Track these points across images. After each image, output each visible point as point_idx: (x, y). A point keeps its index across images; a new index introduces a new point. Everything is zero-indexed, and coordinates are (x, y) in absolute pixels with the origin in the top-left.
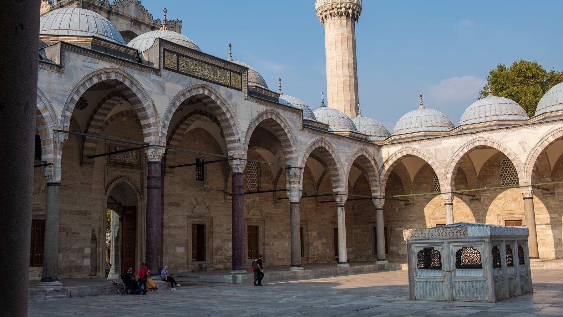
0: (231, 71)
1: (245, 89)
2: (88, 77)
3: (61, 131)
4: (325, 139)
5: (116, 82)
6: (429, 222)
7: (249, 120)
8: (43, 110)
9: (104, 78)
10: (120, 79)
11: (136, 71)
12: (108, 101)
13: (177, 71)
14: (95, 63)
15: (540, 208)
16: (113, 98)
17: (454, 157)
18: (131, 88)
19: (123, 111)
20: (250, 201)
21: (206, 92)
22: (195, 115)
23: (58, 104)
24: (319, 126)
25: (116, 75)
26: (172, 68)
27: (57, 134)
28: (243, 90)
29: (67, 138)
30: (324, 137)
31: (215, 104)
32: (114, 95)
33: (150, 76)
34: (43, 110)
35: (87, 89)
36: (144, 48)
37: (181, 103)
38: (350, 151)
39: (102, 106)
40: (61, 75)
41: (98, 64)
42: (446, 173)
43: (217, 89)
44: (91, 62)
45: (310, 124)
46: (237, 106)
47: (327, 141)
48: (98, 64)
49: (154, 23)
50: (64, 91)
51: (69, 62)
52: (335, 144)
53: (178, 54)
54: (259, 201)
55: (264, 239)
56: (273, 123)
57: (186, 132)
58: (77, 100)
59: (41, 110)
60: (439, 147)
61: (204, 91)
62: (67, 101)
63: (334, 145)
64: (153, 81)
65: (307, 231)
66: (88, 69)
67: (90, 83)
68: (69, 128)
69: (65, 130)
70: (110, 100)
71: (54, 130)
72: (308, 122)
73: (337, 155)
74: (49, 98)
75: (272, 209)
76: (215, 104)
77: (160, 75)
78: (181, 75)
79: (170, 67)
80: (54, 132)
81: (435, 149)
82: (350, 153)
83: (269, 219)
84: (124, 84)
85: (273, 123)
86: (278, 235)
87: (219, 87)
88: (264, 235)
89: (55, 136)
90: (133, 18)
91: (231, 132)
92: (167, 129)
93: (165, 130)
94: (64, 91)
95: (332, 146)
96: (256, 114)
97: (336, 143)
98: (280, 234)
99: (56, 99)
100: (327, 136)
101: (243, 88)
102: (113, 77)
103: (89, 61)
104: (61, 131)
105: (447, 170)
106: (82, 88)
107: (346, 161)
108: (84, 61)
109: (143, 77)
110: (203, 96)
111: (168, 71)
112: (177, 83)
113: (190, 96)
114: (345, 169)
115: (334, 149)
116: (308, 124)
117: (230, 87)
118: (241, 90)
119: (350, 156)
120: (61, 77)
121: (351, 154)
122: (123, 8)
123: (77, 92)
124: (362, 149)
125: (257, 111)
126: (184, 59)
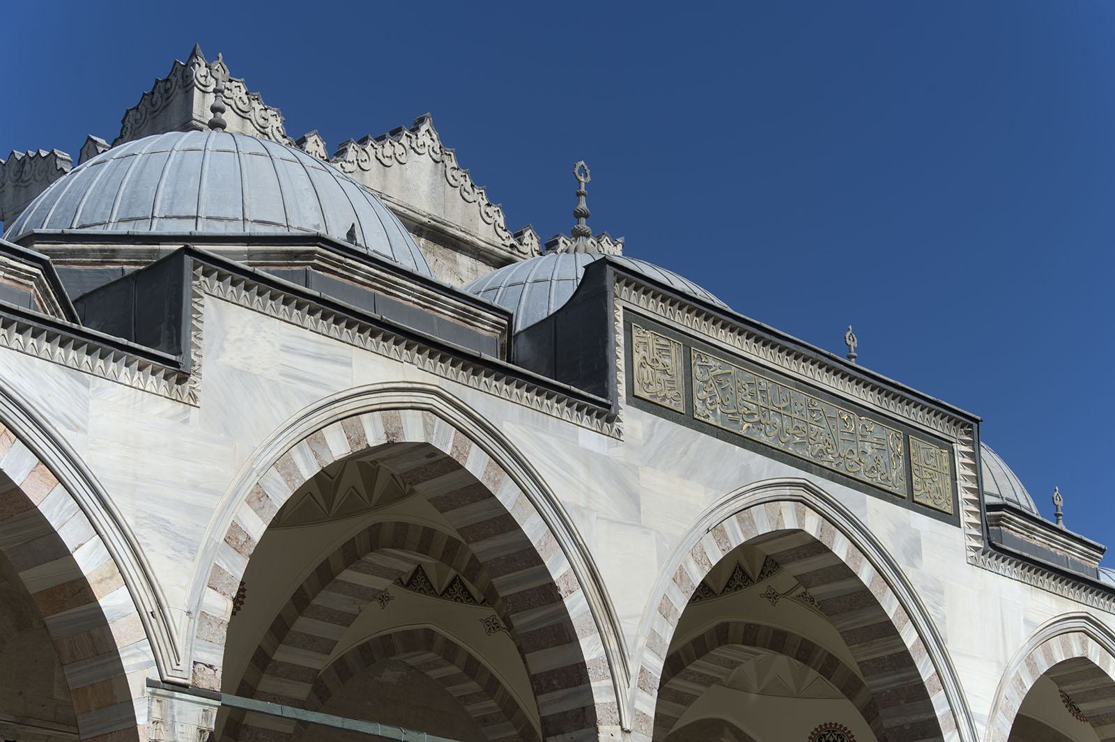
0: (908, 430)
1: (968, 516)
2: (305, 427)
3: (182, 688)
5: (424, 460)
7: (999, 663)
8: (100, 582)
9: (374, 434)
10: (446, 444)
11: (513, 410)
12: (348, 576)
13: (689, 419)
14: (334, 361)
16: (372, 558)
18: (490, 488)
19: (390, 636)
21: (812, 525)
22: (722, 652)
23: (170, 552)
25: (425, 424)
26: (666, 403)
27: (166, 701)
28: (965, 518)
29: (213, 727)
31: (846, 585)
32: (374, 545)
33: (576, 435)
34: (100, 582)
35: (298, 484)
36: (545, 311)
37: (708, 569)
39: (316, 602)
40: (185, 412)
41: (350, 365)
43: (856, 512)
44: (318, 357)
46: (942, 593)
48: (350, 365)
49: (512, 246)
50: (195, 486)
51: (222, 349)
53: (688, 341)
56: (1088, 684)
57: (672, 731)
58: (257, 535)
59: (91, 580)
61: (801, 517)
62: (210, 540)
64: (586, 457)
66: (304, 387)
67: (312, 456)
68: (219, 674)
69: (204, 684)
70: (357, 570)
71: (150, 683)
74: (131, 522)
76: (846, 585)
77: (619, 432)
78: (703, 435)
79: (655, 397)
80: (153, 694)
84: (461, 467)
85: (1088, 684)
87: (864, 502)
89: (156, 715)
90: (426, 220)
91: (923, 717)
92: (656, 693)
93: (646, 696)
94: (195, 486)
96: (1020, 638)
99: (163, 526)
101: (963, 508)
102: (413, 430)
103: (311, 348)
104: (182, 688)
106: (281, 480)
108: (288, 349)
109: (541, 435)
110: (795, 543)
111: (648, 418)
112: (690, 472)
113: (743, 540)
117: (909, 501)
118: (953, 519)
120: (186, 421)
122: (385, 175)
123: (259, 496)
125: (1026, 621)
126: (712, 363)
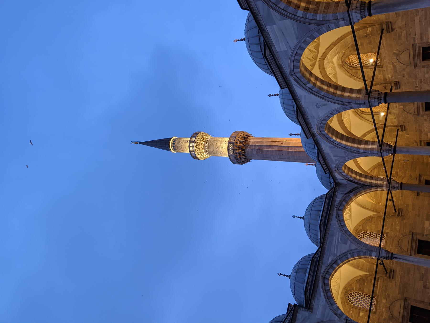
4: (323, 273)
6: (422, 116)
15: (406, 33)
17: (341, 147)
20: (385, 313)
24: (312, 274)
30: (321, 276)
38: (337, 233)
42: (358, 152)
45: (309, 289)
47: (325, 271)
52: (329, 258)
54: (386, 300)
55: (425, 302)
60: (331, 155)
63: (330, 261)
65: (423, 235)
72: (307, 291)
73: (340, 257)
75: (396, 283)
81: (334, 157)
82: (339, 234)
83: (405, 290)
86: (422, 280)
88: (421, 301)
95: (330, 263)
97: (328, 257)
98: (422, 279)
100: (321, 270)
105: (356, 152)
107: (346, 243)
114: (353, 248)
115: (333, 260)
116: (308, 291)
119: (341, 235)
121: (340, 233)
124: (337, 211)
